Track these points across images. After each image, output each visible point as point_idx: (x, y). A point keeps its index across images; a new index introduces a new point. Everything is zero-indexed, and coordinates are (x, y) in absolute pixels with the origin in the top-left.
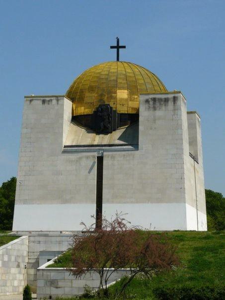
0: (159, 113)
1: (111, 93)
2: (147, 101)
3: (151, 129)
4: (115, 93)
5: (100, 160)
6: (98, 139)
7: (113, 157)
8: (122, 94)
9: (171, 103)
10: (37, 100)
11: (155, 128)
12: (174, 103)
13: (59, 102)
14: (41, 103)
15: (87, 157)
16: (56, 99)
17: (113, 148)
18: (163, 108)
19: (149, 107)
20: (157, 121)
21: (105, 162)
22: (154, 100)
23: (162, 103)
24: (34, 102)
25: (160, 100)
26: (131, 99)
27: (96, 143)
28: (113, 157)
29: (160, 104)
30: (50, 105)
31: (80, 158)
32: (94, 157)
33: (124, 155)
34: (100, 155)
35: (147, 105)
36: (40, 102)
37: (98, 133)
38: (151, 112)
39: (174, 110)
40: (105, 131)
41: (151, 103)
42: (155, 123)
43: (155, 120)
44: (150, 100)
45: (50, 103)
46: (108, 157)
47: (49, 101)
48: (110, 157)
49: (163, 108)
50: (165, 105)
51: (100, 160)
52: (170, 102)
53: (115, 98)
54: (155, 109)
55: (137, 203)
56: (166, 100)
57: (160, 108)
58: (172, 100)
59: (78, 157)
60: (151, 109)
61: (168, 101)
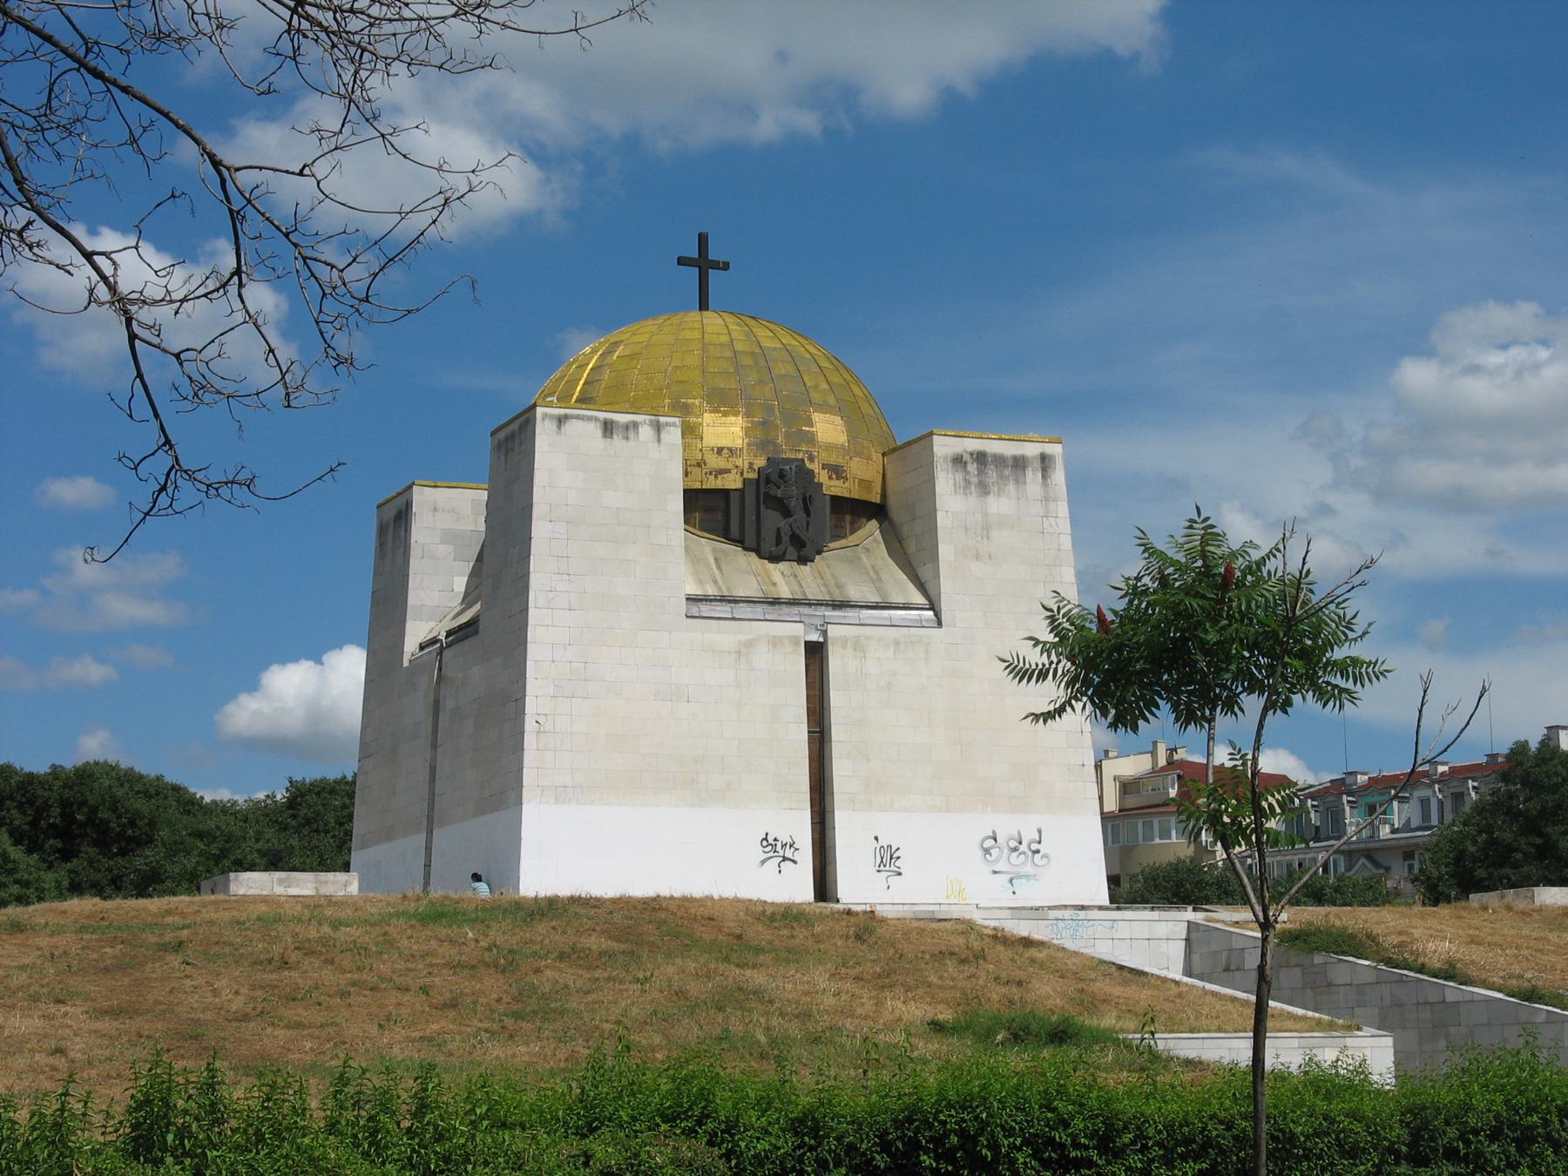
0: (1000, 504)
1: (797, 419)
2: (958, 461)
3: (978, 557)
5: (816, 653)
6: (782, 578)
8: (828, 429)
10: (578, 417)
12: (1044, 477)
14: (599, 432)
15: (775, 642)
16: (651, 423)
17: (886, 613)
19: (967, 482)
20: (994, 533)
21: (837, 663)
22: (981, 458)
23: (1007, 472)
24: (571, 426)
25: (1000, 460)
26: (855, 447)
27: (785, 592)
28: (858, 646)
29: (1001, 476)
30: (632, 443)
31: (750, 644)
32: (794, 640)
33: (897, 643)
34: (815, 637)
35: (959, 476)
36: (595, 430)
37: (775, 559)
40: (801, 550)
41: (972, 468)
43: (986, 528)
44: (967, 457)
45: (631, 435)
46: (844, 647)
47: (627, 427)
49: (1011, 488)
50: (1017, 481)
51: (816, 653)
52: (1029, 473)
53: (811, 439)
54: (984, 489)
56: (1019, 463)
58: (1037, 464)
59: (743, 638)
61: (1024, 468)
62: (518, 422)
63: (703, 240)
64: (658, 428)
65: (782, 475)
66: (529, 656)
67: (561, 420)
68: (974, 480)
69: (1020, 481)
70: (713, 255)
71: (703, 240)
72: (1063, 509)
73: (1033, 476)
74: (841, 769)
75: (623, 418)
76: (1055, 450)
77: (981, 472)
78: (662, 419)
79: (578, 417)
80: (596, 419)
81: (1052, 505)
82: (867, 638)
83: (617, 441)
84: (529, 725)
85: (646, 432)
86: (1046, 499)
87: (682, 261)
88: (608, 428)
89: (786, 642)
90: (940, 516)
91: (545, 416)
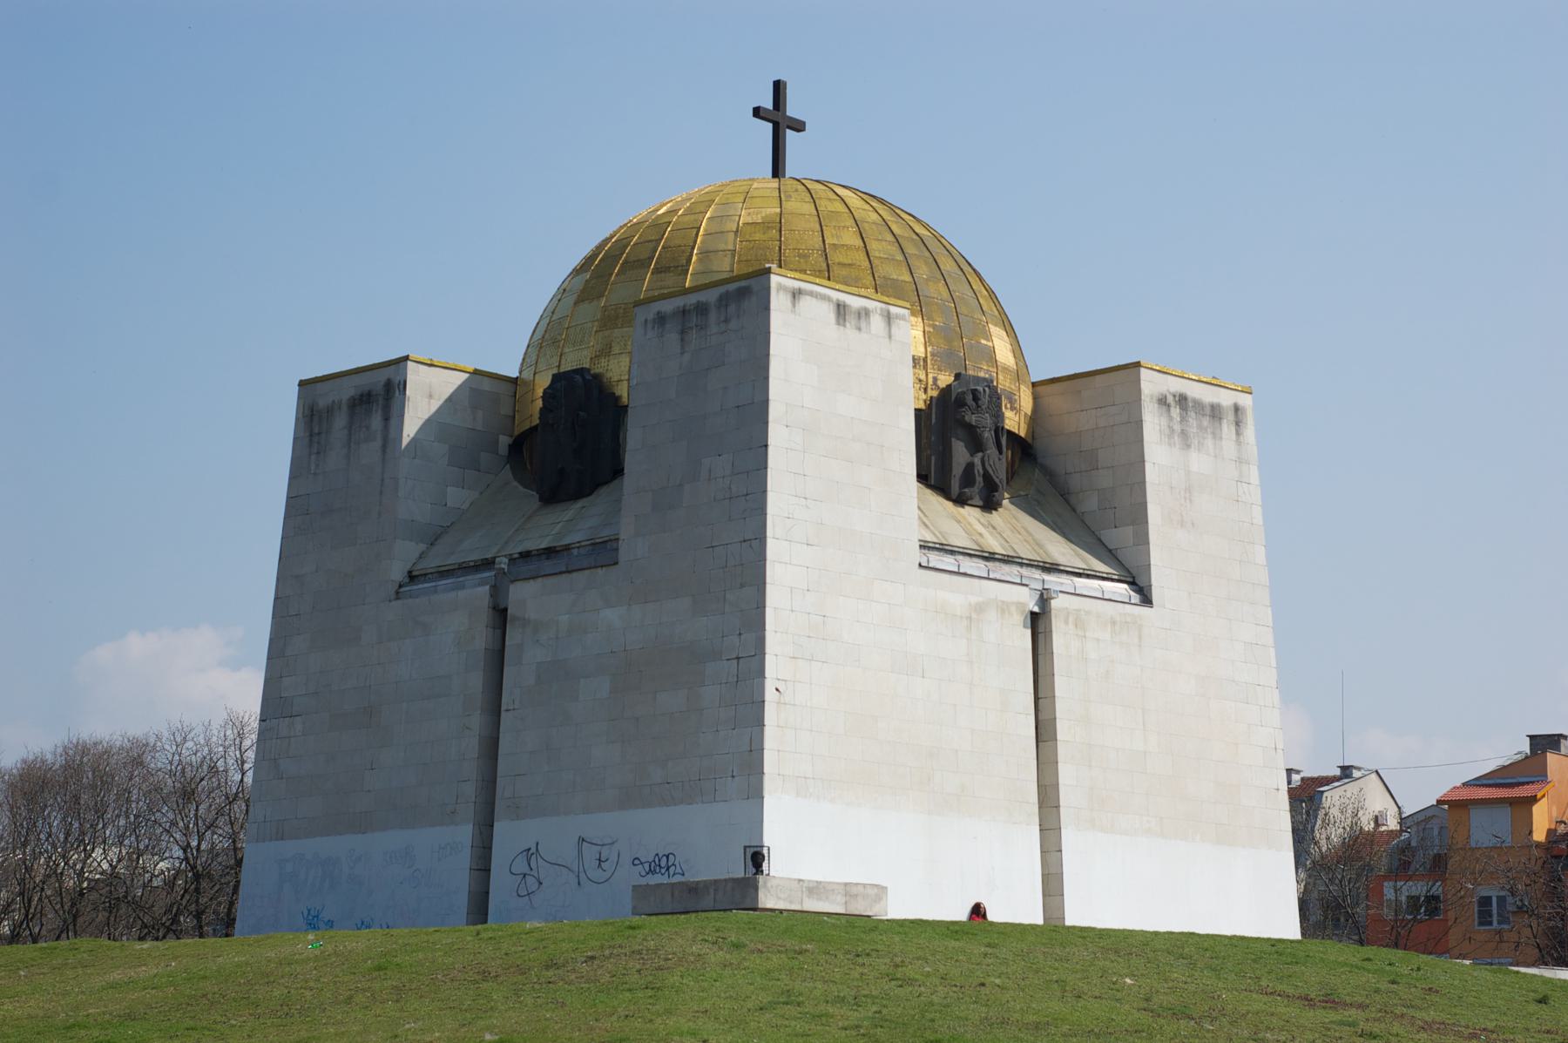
0: (1199, 462)
2: (1162, 401)
3: (1182, 524)
10: (811, 294)
12: (1238, 434)
13: (893, 330)
14: (832, 316)
15: (1003, 608)
21: (1061, 638)
22: (1182, 400)
24: (806, 303)
25: (1199, 406)
29: (1200, 427)
31: (980, 608)
35: (1164, 421)
36: (827, 312)
37: (960, 501)
41: (1176, 412)
44: (1170, 399)
56: (1215, 412)
58: (1231, 417)
59: (974, 599)
62: (722, 289)
63: (778, 87)
64: (889, 318)
65: (976, 398)
66: (768, 603)
67: (796, 295)
68: (1177, 427)
69: (1217, 436)
70: (793, 110)
71: (778, 87)
72: (1254, 474)
73: (1228, 429)
74: (1067, 775)
75: (855, 302)
76: (1245, 401)
77: (1183, 419)
78: (893, 310)
79: (811, 294)
80: (829, 299)
82: (1088, 613)
83: (850, 331)
84: (770, 695)
85: (877, 322)
86: (1240, 461)
87: (757, 112)
88: (841, 310)
89: (1013, 609)
90: (1148, 466)
91: (780, 287)
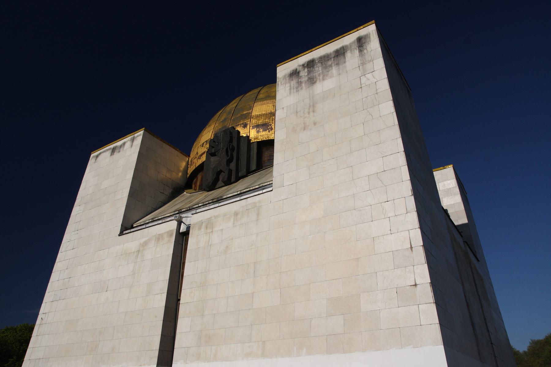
2: (295, 74)
4: (251, 108)
7: (209, 224)
9: (352, 59)
10: (104, 152)
11: (315, 124)
12: (360, 51)
15: (159, 238)
18: (334, 70)
19: (300, 83)
22: (310, 64)
25: (324, 59)
31: (145, 244)
33: (236, 214)
38: (304, 92)
39: (363, 64)
41: (304, 73)
42: (314, 111)
43: (313, 107)
46: (200, 228)
48: (204, 225)
50: (338, 64)
52: (348, 55)
54: (312, 81)
55: (264, 355)
57: (324, 76)
58: (355, 46)
59: (142, 241)
60: (303, 85)
68: (304, 79)
81: (369, 66)
82: (216, 217)
83: (116, 154)
89: (165, 236)
